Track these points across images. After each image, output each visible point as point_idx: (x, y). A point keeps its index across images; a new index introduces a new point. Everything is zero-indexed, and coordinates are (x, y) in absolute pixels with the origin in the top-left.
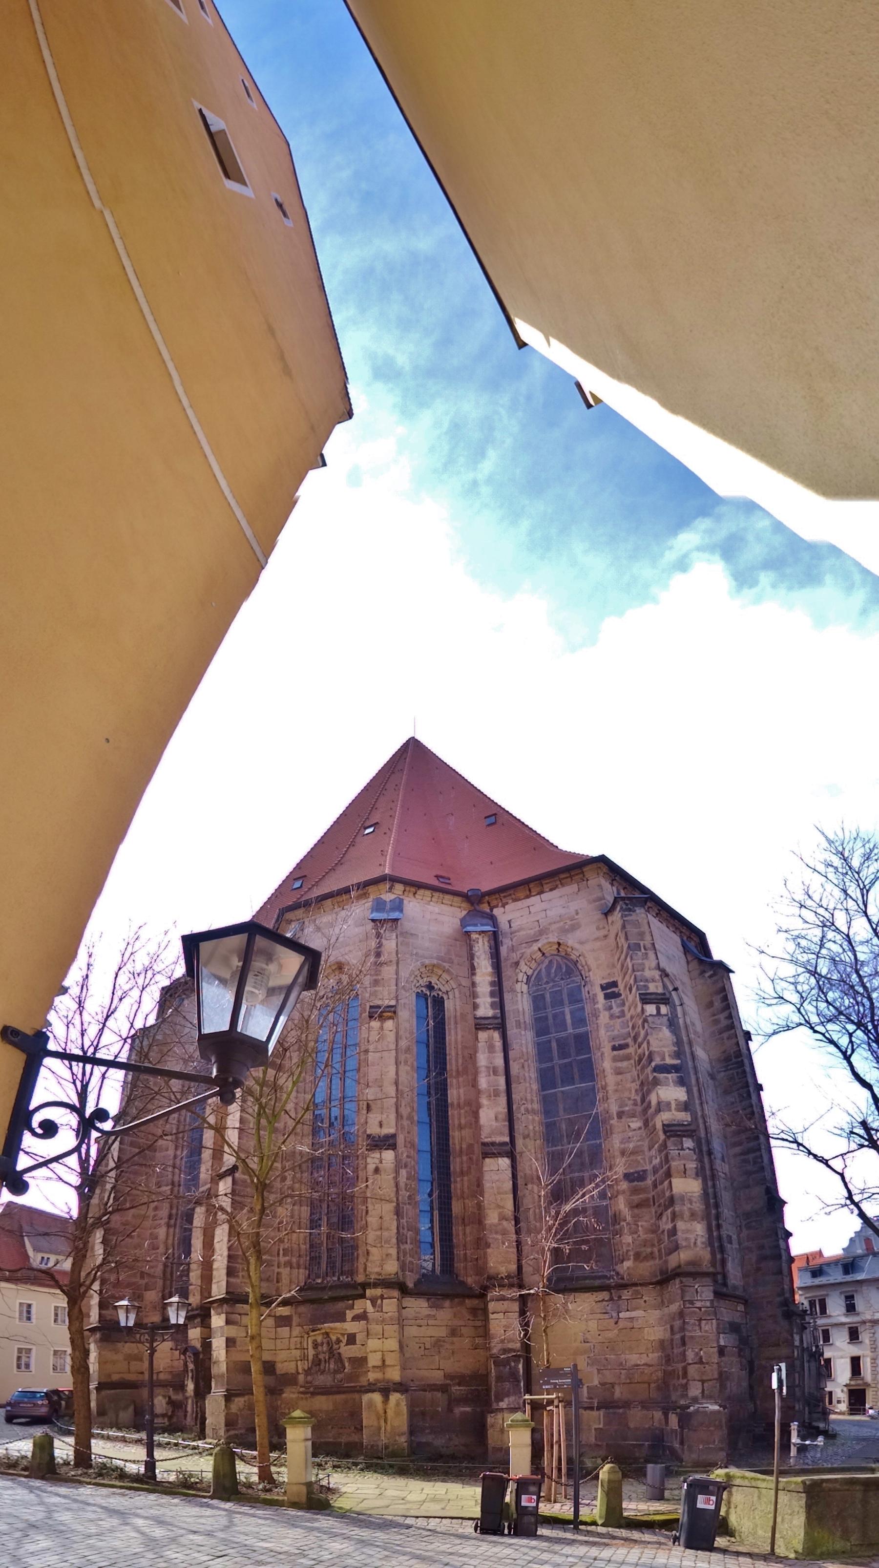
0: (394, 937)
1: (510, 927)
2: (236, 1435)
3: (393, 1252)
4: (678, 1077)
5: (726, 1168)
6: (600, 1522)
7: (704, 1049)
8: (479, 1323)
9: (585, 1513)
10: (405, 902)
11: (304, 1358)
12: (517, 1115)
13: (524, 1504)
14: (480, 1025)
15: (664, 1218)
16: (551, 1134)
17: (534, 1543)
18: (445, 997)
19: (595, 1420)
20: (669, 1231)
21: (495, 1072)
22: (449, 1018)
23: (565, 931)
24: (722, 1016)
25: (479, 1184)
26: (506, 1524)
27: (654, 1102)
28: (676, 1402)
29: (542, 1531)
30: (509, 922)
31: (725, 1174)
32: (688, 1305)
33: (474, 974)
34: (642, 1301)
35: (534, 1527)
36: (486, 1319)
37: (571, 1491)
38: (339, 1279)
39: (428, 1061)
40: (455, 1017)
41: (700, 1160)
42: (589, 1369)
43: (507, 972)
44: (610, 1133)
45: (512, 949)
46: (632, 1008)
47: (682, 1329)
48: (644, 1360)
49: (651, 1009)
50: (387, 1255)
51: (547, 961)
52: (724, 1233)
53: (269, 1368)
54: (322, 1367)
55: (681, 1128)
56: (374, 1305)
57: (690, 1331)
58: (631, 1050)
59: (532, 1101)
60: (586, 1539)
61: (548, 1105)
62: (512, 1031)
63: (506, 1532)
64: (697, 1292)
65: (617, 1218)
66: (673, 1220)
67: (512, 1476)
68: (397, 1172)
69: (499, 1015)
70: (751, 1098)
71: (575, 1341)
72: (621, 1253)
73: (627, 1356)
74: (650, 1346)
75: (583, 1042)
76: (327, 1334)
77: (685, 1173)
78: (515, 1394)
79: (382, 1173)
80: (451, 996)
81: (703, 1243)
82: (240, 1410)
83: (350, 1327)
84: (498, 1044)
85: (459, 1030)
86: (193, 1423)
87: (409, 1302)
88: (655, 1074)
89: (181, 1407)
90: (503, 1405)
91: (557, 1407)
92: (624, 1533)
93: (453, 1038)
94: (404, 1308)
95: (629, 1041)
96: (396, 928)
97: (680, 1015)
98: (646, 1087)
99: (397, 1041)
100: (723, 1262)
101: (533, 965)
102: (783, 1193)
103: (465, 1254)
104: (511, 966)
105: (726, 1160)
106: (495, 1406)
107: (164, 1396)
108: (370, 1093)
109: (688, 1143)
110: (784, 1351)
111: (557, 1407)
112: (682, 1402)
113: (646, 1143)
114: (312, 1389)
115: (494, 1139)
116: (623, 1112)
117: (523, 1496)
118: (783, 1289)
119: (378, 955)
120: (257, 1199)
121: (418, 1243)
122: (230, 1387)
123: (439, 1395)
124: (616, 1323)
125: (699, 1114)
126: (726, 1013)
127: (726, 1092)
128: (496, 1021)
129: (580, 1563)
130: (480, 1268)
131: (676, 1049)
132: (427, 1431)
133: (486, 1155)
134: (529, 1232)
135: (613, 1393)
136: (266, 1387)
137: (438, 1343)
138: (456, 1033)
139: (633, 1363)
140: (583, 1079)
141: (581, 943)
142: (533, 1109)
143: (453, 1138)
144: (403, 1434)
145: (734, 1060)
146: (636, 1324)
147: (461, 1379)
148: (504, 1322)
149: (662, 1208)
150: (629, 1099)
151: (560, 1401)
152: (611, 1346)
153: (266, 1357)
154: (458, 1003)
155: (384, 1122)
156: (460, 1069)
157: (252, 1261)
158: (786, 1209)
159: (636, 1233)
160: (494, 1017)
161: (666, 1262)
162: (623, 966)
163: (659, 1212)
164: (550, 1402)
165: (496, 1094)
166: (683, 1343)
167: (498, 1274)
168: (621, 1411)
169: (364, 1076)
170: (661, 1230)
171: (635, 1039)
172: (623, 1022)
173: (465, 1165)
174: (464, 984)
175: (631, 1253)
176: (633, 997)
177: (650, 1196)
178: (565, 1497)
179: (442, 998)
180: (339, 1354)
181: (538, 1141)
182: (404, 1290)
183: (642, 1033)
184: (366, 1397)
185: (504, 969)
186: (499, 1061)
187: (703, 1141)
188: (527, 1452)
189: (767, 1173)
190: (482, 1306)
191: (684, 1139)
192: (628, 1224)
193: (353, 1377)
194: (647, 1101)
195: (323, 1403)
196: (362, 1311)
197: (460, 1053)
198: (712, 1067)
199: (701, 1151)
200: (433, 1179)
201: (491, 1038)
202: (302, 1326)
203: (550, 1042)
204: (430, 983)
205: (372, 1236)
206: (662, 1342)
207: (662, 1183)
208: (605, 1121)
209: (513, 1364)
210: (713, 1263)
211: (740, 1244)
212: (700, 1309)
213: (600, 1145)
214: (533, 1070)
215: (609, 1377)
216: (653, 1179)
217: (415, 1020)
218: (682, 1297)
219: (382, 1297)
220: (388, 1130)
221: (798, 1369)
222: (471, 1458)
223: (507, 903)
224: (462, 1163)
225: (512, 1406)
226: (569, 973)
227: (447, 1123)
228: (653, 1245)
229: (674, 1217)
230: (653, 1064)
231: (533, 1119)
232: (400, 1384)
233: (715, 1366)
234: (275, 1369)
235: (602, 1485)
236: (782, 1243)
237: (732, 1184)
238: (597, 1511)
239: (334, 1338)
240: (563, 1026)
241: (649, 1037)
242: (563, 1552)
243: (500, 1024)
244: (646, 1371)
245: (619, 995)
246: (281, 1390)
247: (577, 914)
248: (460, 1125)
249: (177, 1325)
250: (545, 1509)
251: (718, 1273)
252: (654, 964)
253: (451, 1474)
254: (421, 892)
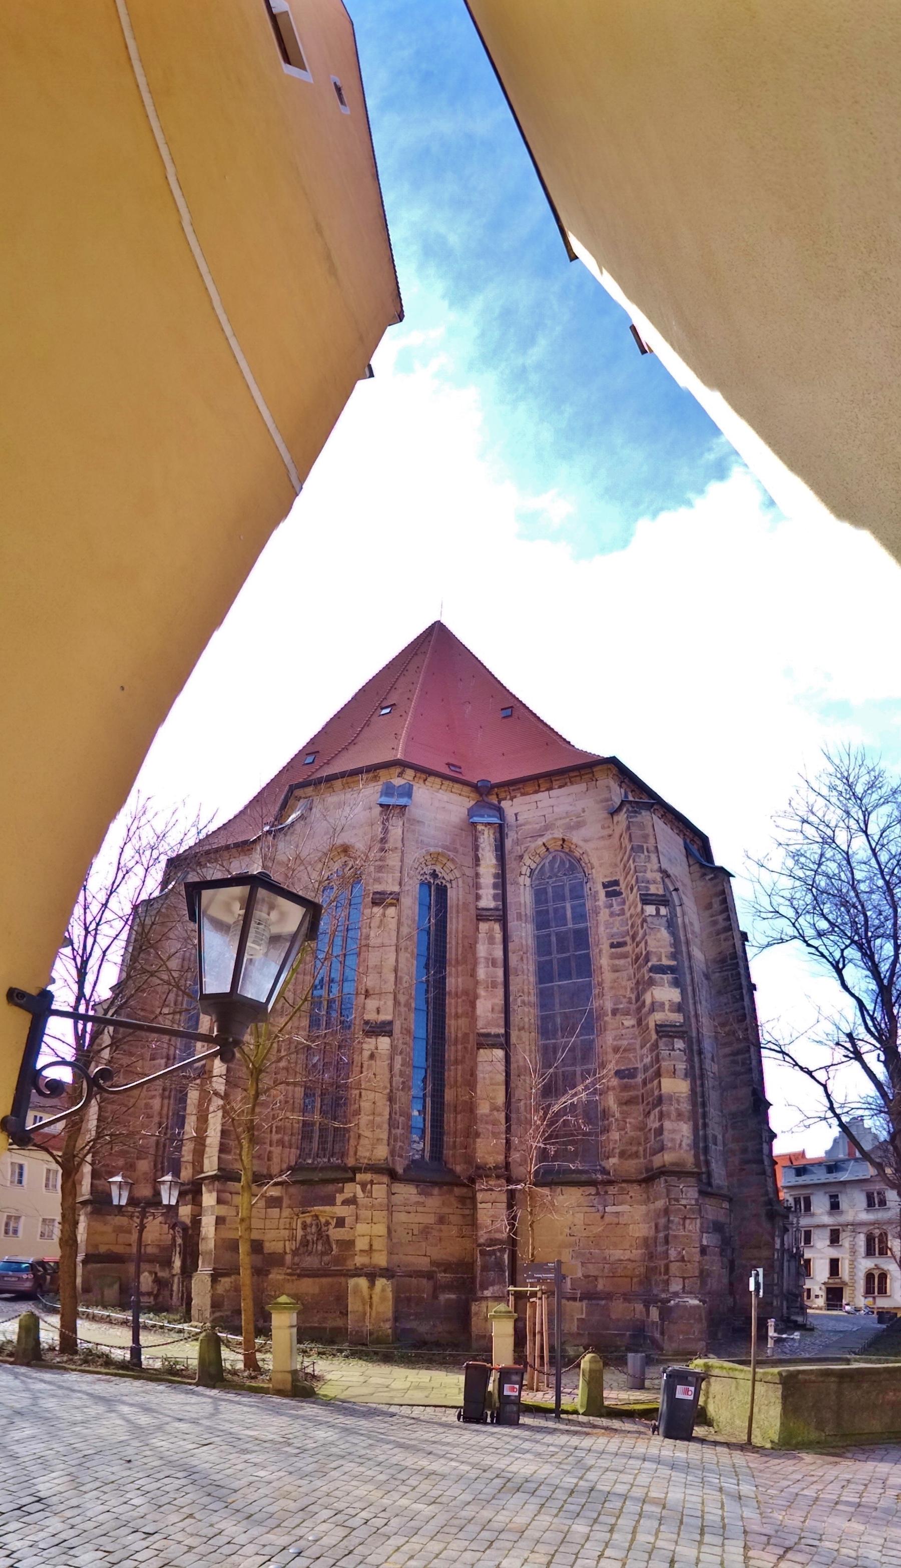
0: (401, 823)
1: (517, 820)
2: (222, 1317)
3: (385, 1136)
4: (673, 978)
5: (715, 1068)
6: (581, 1411)
7: (701, 950)
8: (467, 1212)
9: (567, 1402)
10: (415, 788)
11: (293, 1238)
12: (513, 1007)
13: (506, 1393)
14: (482, 916)
15: (652, 1116)
16: (545, 1029)
17: (516, 1432)
18: (449, 886)
19: (577, 1310)
20: (655, 1129)
21: (494, 963)
22: (452, 907)
23: (570, 828)
24: (720, 918)
25: (473, 1073)
26: (489, 1413)
27: (648, 1002)
28: (657, 1295)
29: (524, 1420)
30: (516, 815)
31: (714, 1073)
32: (673, 1202)
33: (478, 865)
34: (628, 1197)
35: (516, 1416)
36: (475, 1208)
37: (553, 1379)
38: (329, 1160)
39: (428, 949)
40: (458, 905)
41: (690, 1060)
42: (573, 1262)
43: (511, 864)
44: (603, 1030)
45: (517, 842)
46: (632, 908)
47: (667, 1228)
48: (628, 1255)
49: (650, 910)
50: (378, 1140)
51: (550, 857)
52: (710, 1132)
53: (257, 1247)
54: (310, 1248)
55: (673, 1029)
56: (363, 1191)
57: (674, 1230)
58: (628, 948)
59: (529, 993)
60: (567, 1427)
61: (545, 998)
62: (512, 924)
63: (489, 1420)
64: (682, 1192)
65: (605, 1114)
66: (660, 1119)
67: (495, 1365)
68: (392, 1059)
69: (501, 907)
70: (743, 1000)
71: (561, 1234)
72: (607, 1149)
73: (612, 1252)
75: (582, 938)
76: (317, 1216)
77: (674, 1073)
78: (499, 1283)
79: (378, 1059)
80: (454, 885)
81: (688, 1145)
82: (227, 1291)
83: (340, 1211)
84: (499, 936)
85: (460, 919)
86: (178, 1303)
87: (399, 1188)
88: (651, 974)
89: (167, 1286)
90: (487, 1293)
91: (540, 1299)
92: (605, 1422)
93: (454, 927)
94: (393, 1194)
95: (628, 939)
96: (403, 815)
97: (679, 914)
98: (642, 986)
99: (398, 928)
100: (707, 1163)
101: (537, 859)
102: (769, 1096)
103: (455, 1142)
104: (515, 859)
105: (715, 1059)
106: (479, 1294)
107: (150, 1273)
108: (370, 981)
109: (679, 1044)
110: (765, 1253)
111: (540, 1299)
112: (663, 1296)
113: (638, 1042)
114: (298, 1271)
115: (489, 1030)
116: (618, 1009)
117: (506, 1386)
118: (767, 1191)
119: (383, 840)
120: (252, 1084)
121: (410, 1128)
122: (216, 1266)
123: (424, 1281)
124: (602, 1217)
125: (693, 1013)
126: (724, 916)
127: (719, 993)
128: (498, 913)
129: (561, 1453)
130: (469, 1159)
131: (673, 950)
132: (412, 1317)
133: (480, 1046)
134: (519, 1122)
135: (596, 1286)
136: (252, 1268)
137: (426, 1231)
138: (458, 922)
139: (617, 1258)
140: (579, 975)
141: (586, 841)
142: (529, 1002)
143: (449, 1027)
144: (387, 1320)
145: (729, 962)
146: (622, 1220)
147: (447, 1267)
148: (491, 1212)
149: (650, 1106)
150: (625, 997)
151: (543, 1293)
152: (596, 1240)
153: (255, 1235)
154: (460, 893)
155: (382, 1009)
156: (460, 958)
157: (245, 1143)
158: (771, 1111)
159: (624, 1129)
160: (496, 909)
161: (651, 1161)
162: (625, 866)
163: (647, 1110)
164: (534, 1294)
165: (494, 985)
166: (667, 1242)
167: (487, 1164)
168: (603, 1302)
169: (364, 961)
170: (648, 1127)
171: (633, 938)
172: (622, 920)
173: (459, 1054)
174: (467, 874)
175: (617, 1151)
176: (633, 897)
177: (640, 1093)
178: (548, 1386)
179: (446, 886)
180: (328, 1236)
181: (533, 1034)
182: (393, 1176)
183: (641, 932)
184: (352, 1282)
185: (508, 861)
186: (499, 953)
187: (694, 1040)
188: (510, 1342)
189: (755, 1075)
190: (470, 1195)
191: (676, 1040)
192: (616, 1120)
193: (340, 1260)
194: (642, 999)
195: (309, 1286)
196: (352, 1195)
197: (460, 942)
198: (707, 967)
199: (691, 1050)
200: (428, 1067)
201: (491, 930)
202: (292, 1208)
203: (549, 935)
204: (435, 871)
205: (364, 1119)
206: (646, 1239)
207: (652, 1081)
208: (598, 1018)
209: (498, 1254)
210: (697, 1164)
211: (724, 1145)
212: (685, 1206)
213: (593, 1040)
214: (531, 962)
215: (592, 1270)
216: (643, 1077)
217: (417, 907)
218: (668, 1196)
219: (372, 1183)
220: (386, 1017)
221: (777, 1270)
222: (455, 1346)
223: (515, 797)
224: (456, 1051)
225: (497, 1295)
226: (572, 868)
227: (444, 1011)
228: (640, 1144)
229: (661, 1116)
230: (650, 964)
231: (529, 1011)
232: (387, 1269)
233: (697, 1264)
234: (262, 1248)
235: (583, 1375)
236: (765, 1146)
237: (720, 1084)
238: (578, 1400)
239: (323, 1220)
240: (563, 920)
241: (647, 937)
242: (545, 1441)
243: (501, 916)
245: (620, 893)
246: (268, 1271)
247: (584, 812)
248: (456, 1014)
249: (169, 1207)
250: (528, 1398)
251: (703, 1173)
252: (656, 867)
253: (435, 1361)
254: (431, 779)
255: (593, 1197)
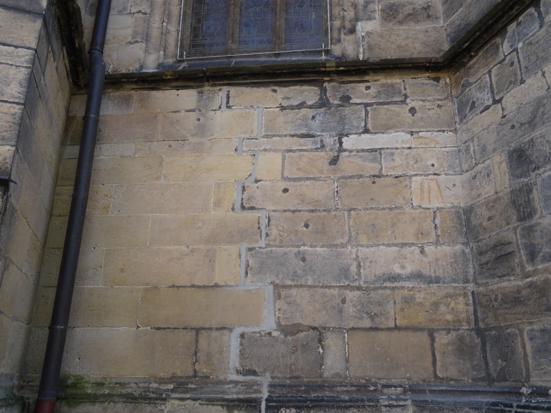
71: (218, 204)
73: (364, 251)
74: (428, 225)
139: (379, 271)
244: (419, 297)
255: (310, 113)
